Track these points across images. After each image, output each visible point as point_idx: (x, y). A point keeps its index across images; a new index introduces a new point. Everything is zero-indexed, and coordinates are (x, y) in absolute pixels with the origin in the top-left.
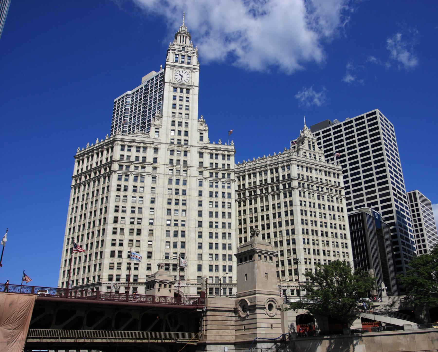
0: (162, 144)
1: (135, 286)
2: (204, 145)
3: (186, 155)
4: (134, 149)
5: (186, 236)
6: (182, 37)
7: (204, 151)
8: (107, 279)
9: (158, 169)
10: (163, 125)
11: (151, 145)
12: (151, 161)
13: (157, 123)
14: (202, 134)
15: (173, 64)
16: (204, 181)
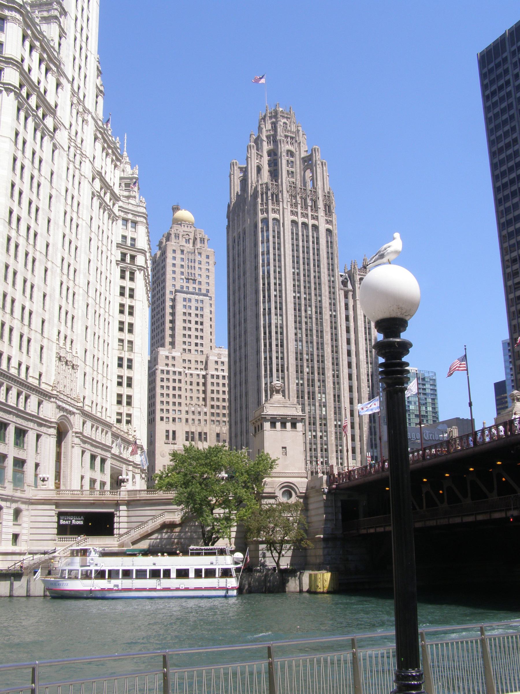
0: (65, 79)
16: (95, 199)
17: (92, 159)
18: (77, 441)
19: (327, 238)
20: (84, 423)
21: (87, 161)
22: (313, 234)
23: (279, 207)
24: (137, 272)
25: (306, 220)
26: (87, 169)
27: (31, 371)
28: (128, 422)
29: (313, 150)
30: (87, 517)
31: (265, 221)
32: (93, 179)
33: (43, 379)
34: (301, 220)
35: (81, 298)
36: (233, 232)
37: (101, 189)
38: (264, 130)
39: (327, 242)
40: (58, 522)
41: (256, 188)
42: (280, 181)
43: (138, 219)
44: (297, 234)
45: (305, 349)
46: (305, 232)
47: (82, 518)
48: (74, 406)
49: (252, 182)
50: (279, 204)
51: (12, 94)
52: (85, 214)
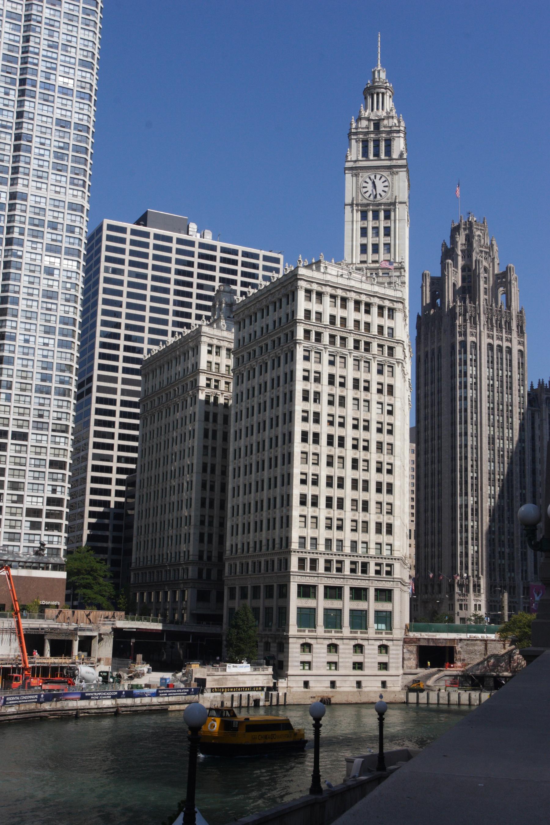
19: (519, 359)
22: (506, 356)
23: (476, 329)
25: (500, 343)
29: (508, 269)
31: (463, 344)
34: (496, 343)
36: (426, 345)
38: (459, 243)
39: (519, 363)
41: (454, 307)
42: (477, 303)
44: (493, 357)
45: (497, 469)
46: (499, 354)
49: (449, 301)
50: (476, 327)
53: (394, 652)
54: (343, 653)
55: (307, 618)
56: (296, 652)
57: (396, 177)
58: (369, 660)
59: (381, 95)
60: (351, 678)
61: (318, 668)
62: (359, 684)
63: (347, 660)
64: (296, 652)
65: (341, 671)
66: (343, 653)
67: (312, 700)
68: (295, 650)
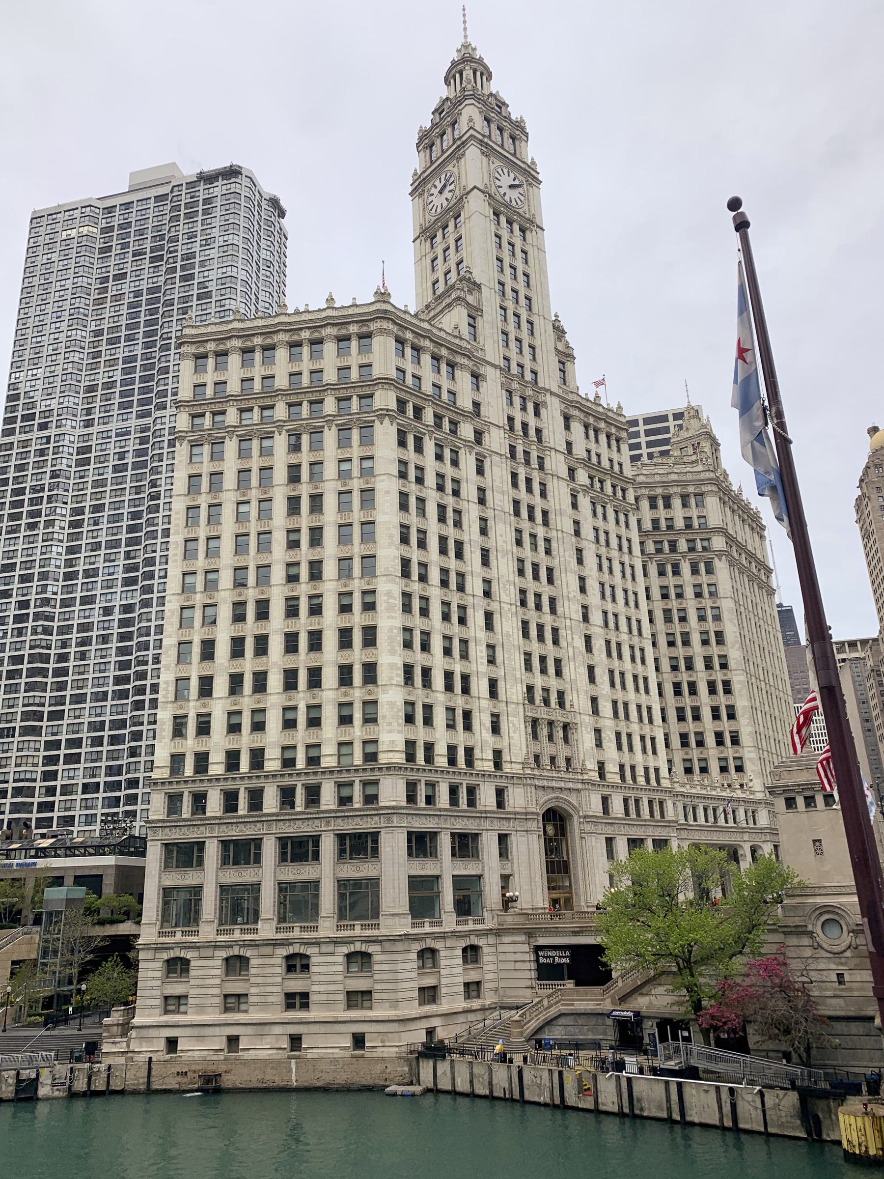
0: (489, 368)
1: (473, 781)
2: (571, 397)
3: (537, 414)
4: (426, 359)
5: (563, 643)
6: (478, 74)
7: (575, 412)
8: (404, 756)
9: (486, 437)
10: (484, 309)
11: (465, 361)
12: (469, 407)
13: (470, 299)
14: (563, 364)
15: (486, 140)
16: (580, 497)
17: (563, 447)
18: (587, 827)
20: (605, 800)
21: (553, 453)
24: (716, 560)
26: (557, 464)
27: (477, 753)
28: (739, 769)
30: (574, 950)
32: (572, 471)
33: (505, 757)
35: (569, 632)
37: (591, 478)
40: (537, 961)
43: (704, 489)
47: (568, 953)
48: (577, 781)
51: (387, 418)
52: (563, 522)
53: (385, 967)
54: (258, 975)
55: (183, 907)
56: (153, 979)
57: (462, 160)
58: (322, 988)
59: (458, 76)
60: (277, 1030)
61: (201, 1009)
62: (295, 1041)
63: (269, 989)
64: (153, 979)
65: (255, 1015)
66: (258, 975)
67: (179, 1079)
68: (150, 974)
